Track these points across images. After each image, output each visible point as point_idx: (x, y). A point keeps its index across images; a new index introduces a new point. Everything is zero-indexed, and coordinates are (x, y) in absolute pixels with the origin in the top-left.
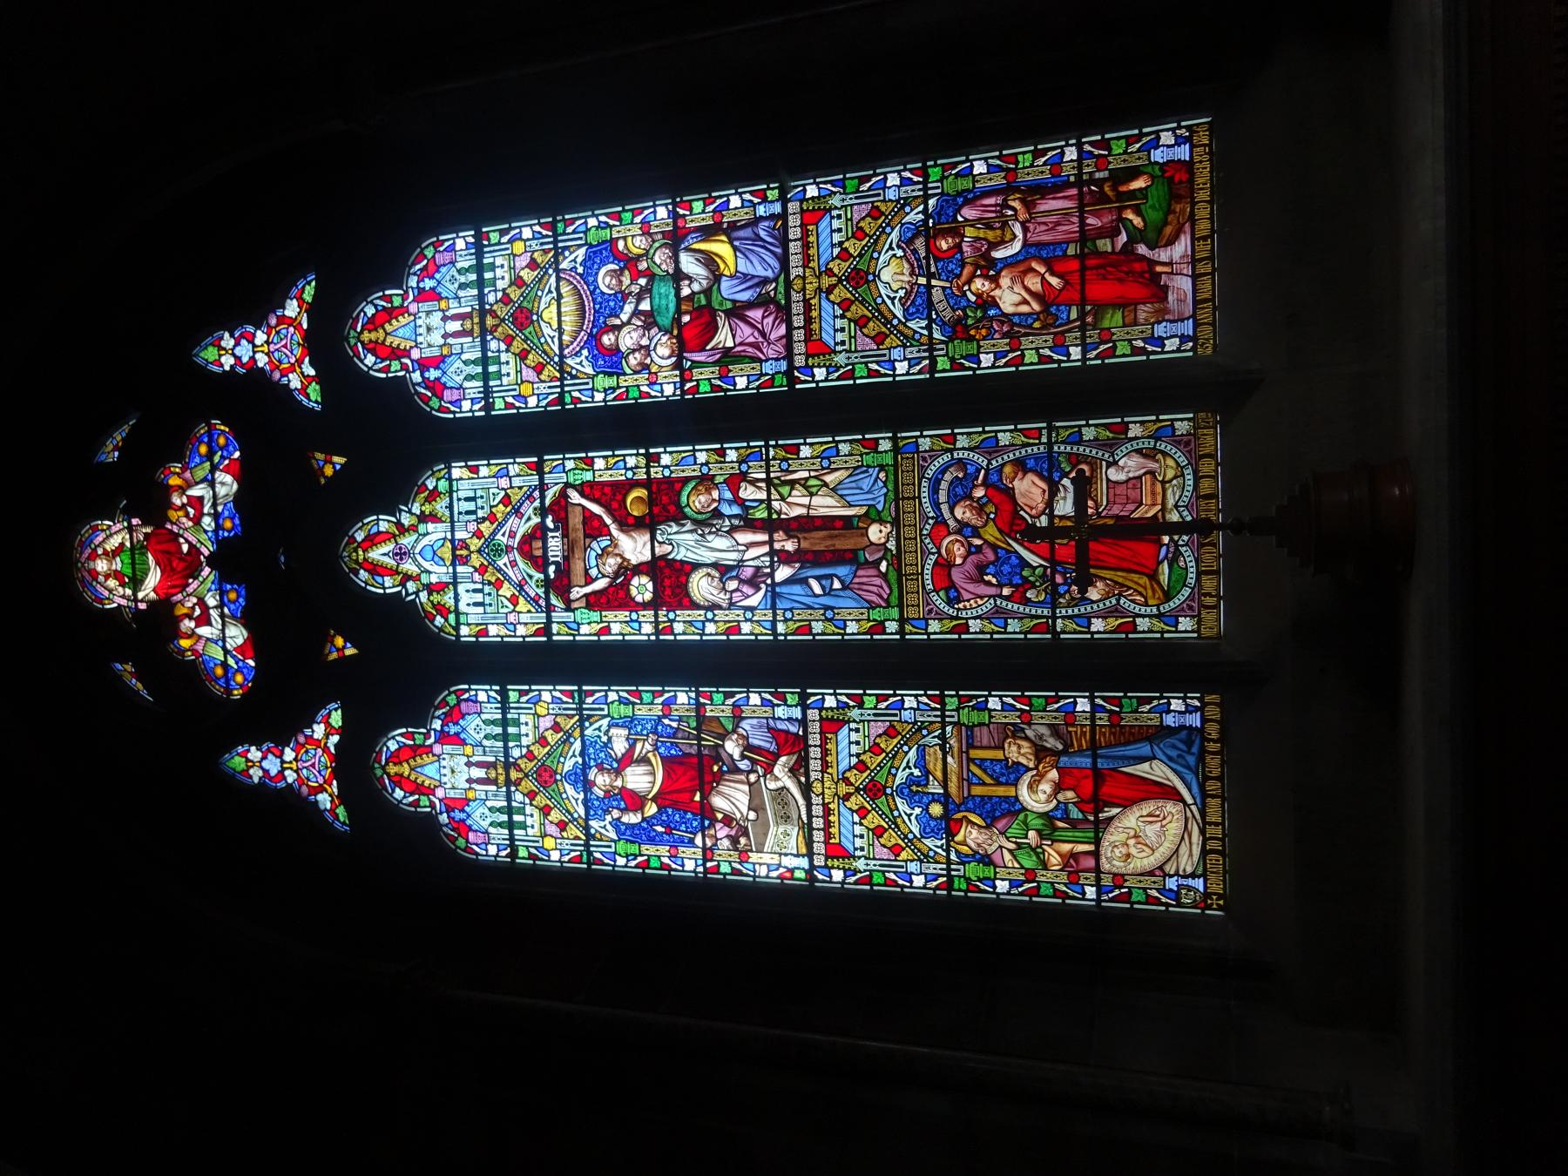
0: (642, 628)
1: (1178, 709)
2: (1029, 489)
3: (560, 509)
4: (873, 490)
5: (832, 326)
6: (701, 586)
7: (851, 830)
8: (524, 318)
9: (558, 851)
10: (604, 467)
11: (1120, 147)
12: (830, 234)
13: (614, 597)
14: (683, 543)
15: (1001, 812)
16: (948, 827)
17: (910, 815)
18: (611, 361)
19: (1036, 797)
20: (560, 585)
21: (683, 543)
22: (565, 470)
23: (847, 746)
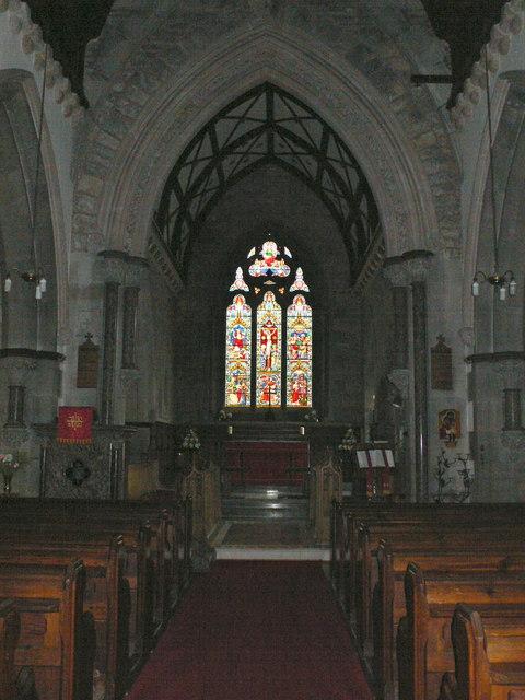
0: (258, 338)
1: (249, 403)
2: (273, 387)
3: (274, 327)
4: (274, 369)
5: (294, 365)
6: (264, 346)
7: (233, 365)
8: (299, 322)
9: (229, 323)
10: (280, 333)
11: (310, 398)
12: (305, 365)
13: (263, 334)
14: (269, 343)
15: (236, 382)
16: (234, 376)
17: (236, 371)
18: (292, 335)
19: (238, 387)
20: (264, 326)
21: (269, 343)
22: (279, 328)
23: (244, 364)
